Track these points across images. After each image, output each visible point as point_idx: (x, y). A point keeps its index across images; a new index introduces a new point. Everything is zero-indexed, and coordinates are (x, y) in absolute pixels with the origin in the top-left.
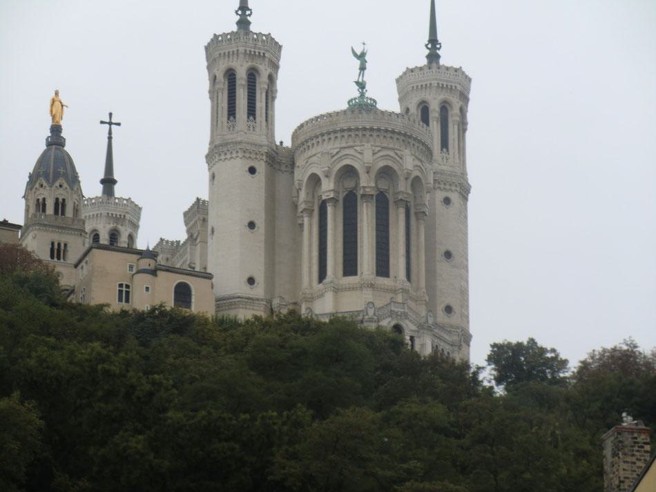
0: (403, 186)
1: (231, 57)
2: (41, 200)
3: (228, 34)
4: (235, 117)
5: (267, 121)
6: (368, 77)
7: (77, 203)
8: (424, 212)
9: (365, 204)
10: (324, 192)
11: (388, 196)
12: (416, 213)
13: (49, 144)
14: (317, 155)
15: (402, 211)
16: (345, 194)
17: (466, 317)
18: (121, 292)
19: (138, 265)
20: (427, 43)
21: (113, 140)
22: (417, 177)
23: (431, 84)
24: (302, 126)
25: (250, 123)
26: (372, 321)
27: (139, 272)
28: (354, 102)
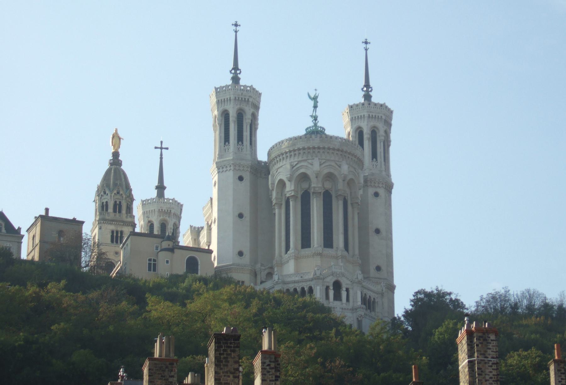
0: (341, 185)
1: (226, 102)
2: (105, 204)
3: (224, 87)
4: (229, 143)
5: (251, 144)
6: (319, 112)
7: (129, 203)
8: (357, 203)
9: (315, 199)
10: (288, 192)
11: (331, 192)
12: (352, 204)
13: (111, 164)
14: (283, 166)
15: (341, 203)
16: (302, 193)
17: (391, 274)
18: (150, 264)
19: (161, 246)
20: (363, 87)
21: (163, 159)
22: (352, 180)
23: (364, 115)
24: (273, 147)
25: (239, 146)
26: (319, 279)
27: (162, 250)
28: (309, 129)
